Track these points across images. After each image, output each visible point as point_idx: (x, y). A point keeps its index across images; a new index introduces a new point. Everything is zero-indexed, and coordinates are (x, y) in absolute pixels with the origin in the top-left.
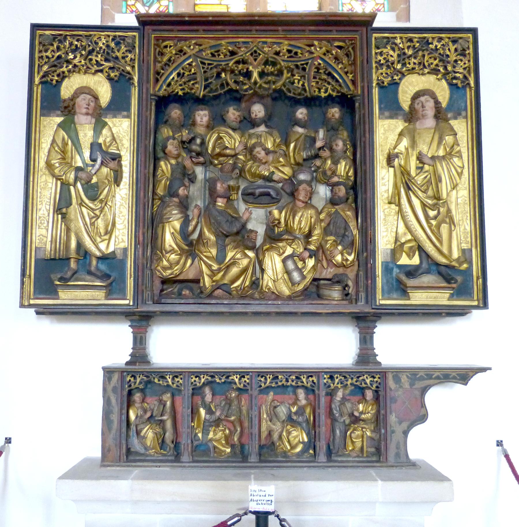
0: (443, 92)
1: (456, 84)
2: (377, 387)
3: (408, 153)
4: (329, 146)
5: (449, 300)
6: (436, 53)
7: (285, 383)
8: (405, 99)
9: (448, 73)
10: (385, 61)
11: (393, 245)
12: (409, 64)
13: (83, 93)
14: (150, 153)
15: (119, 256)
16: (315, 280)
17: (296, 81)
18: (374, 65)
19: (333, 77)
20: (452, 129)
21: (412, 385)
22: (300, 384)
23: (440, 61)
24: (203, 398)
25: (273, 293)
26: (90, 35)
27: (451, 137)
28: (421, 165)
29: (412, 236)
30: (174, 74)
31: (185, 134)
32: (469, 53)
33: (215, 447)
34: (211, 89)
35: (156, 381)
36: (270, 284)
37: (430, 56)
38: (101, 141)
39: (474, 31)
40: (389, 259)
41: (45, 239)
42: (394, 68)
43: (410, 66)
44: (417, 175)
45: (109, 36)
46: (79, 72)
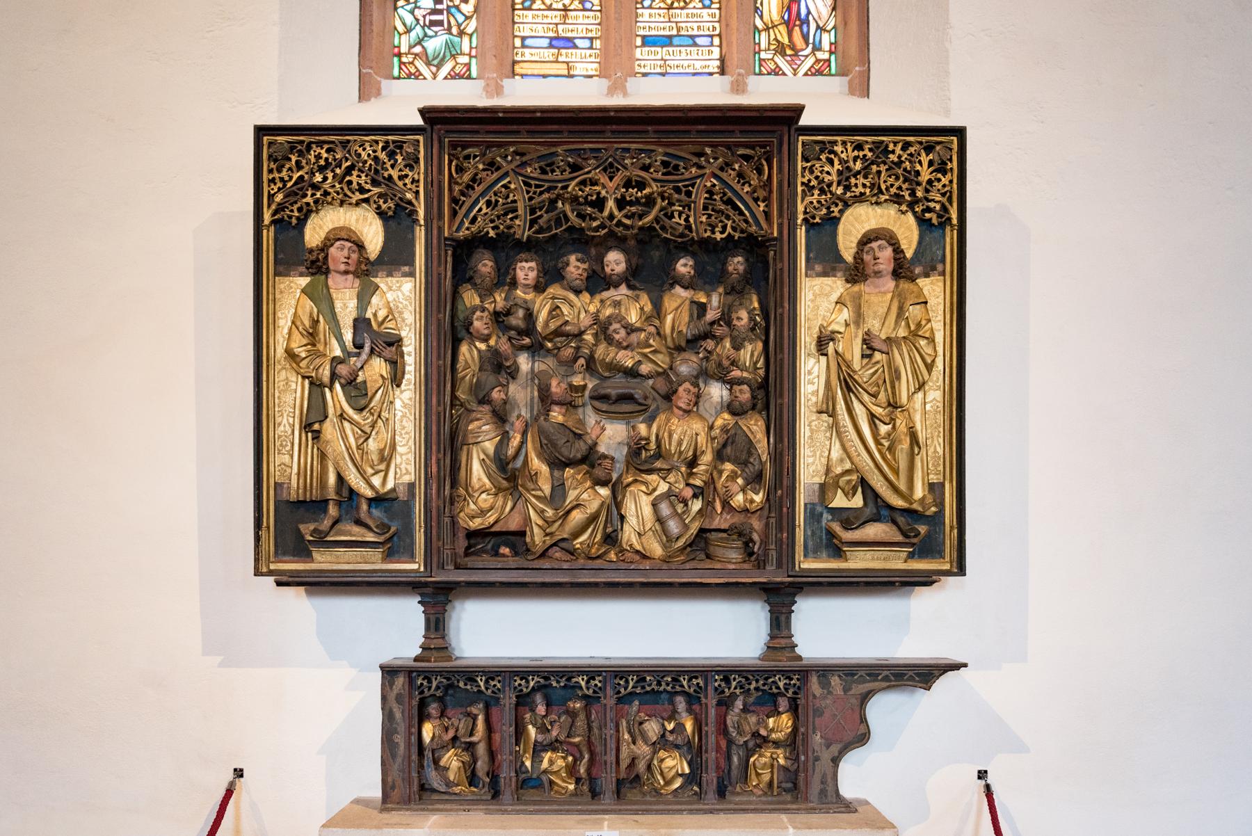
0: (907, 231)
1: (930, 219)
2: (795, 693)
4: (726, 318)
7: (656, 688)
8: (847, 245)
13: (339, 239)
14: (447, 330)
15: (402, 494)
16: (702, 531)
17: (676, 214)
18: (800, 189)
19: (736, 208)
21: (846, 690)
22: (678, 688)
23: (904, 182)
24: (533, 710)
25: (638, 552)
26: (348, 141)
30: (482, 203)
31: (500, 300)
33: (551, 782)
34: (541, 228)
35: (461, 684)
36: (634, 540)
38: (369, 315)
39: (960, 132)
41: (289, 470)
45: (377, 142)
46: (331, 204)
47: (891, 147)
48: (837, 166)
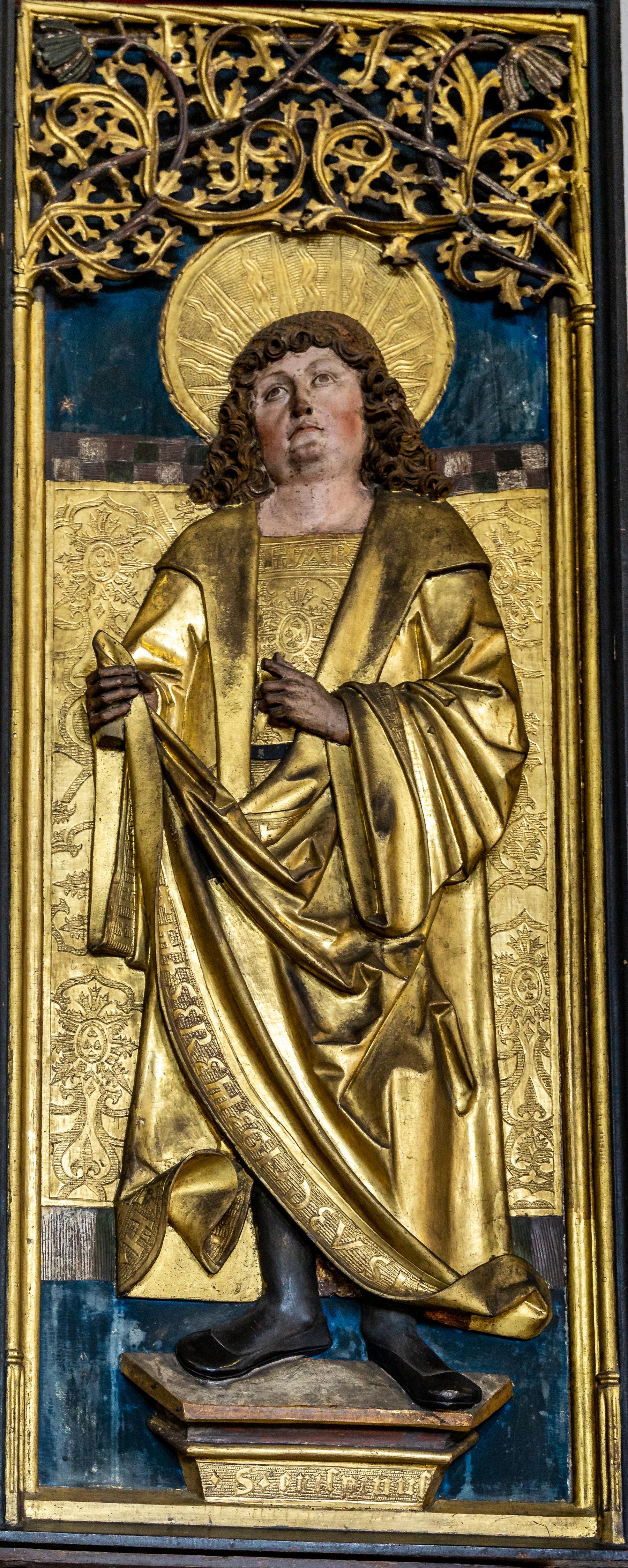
1: (496, 290)
3: (205, 671)
5: (427, 1507)
6: (383, 115)
9: (446, 233)
10: (85, 154)
11: (111, 1190)
12: (227, 172)
18: (24, 175)
20: (462, 535)
23: (399, 162)
27: (455, 581)
28: (280, 737)
29: (220, 1134)
32: (568, 122)
37: (345, 131)
40: (85, 1271)
42: (137, 192)
43: (231, 188)
44: (255, 791)
47: (349, 43)
48: (157, 104)
